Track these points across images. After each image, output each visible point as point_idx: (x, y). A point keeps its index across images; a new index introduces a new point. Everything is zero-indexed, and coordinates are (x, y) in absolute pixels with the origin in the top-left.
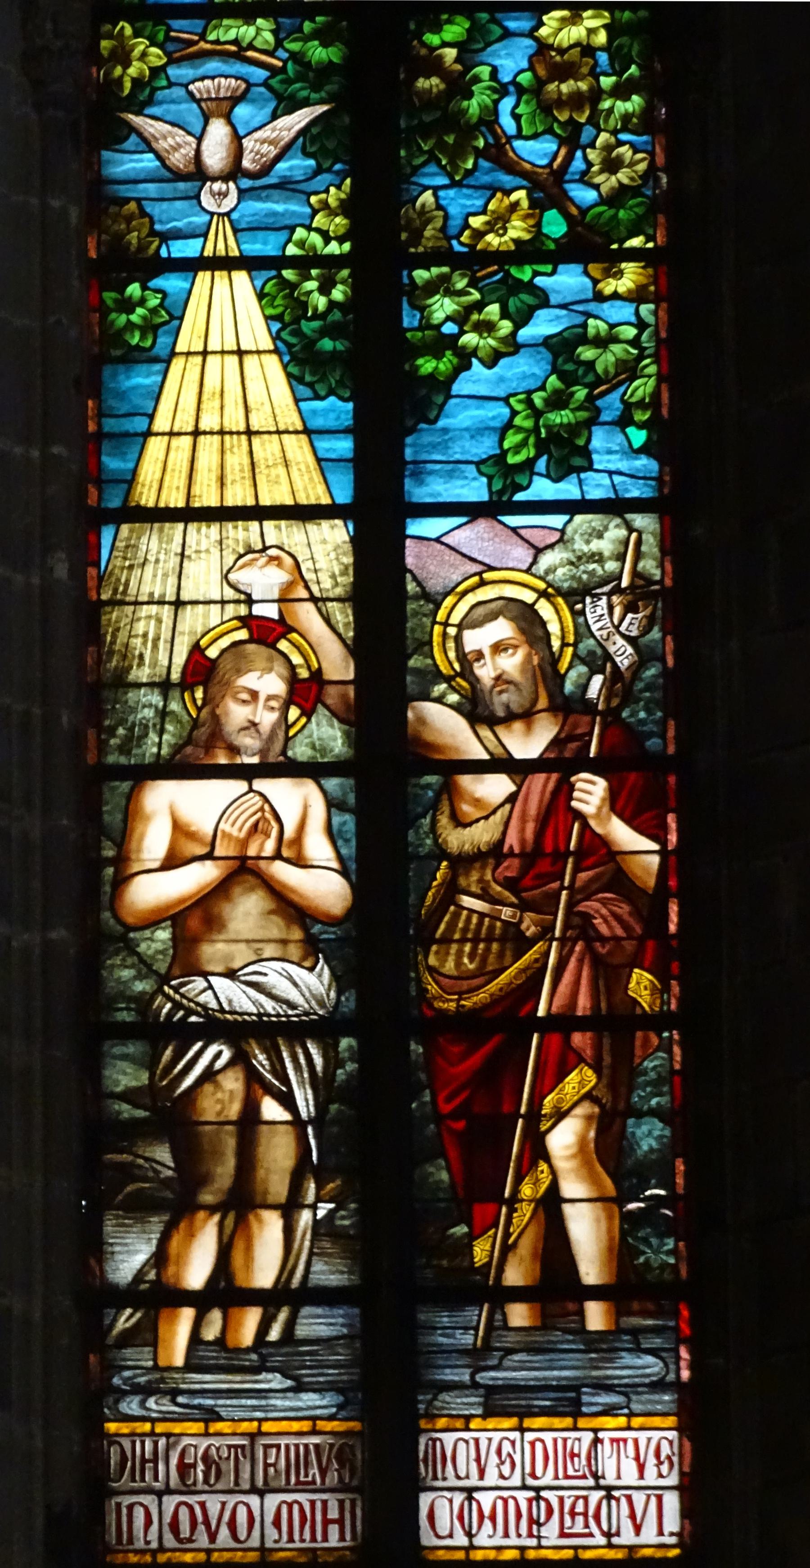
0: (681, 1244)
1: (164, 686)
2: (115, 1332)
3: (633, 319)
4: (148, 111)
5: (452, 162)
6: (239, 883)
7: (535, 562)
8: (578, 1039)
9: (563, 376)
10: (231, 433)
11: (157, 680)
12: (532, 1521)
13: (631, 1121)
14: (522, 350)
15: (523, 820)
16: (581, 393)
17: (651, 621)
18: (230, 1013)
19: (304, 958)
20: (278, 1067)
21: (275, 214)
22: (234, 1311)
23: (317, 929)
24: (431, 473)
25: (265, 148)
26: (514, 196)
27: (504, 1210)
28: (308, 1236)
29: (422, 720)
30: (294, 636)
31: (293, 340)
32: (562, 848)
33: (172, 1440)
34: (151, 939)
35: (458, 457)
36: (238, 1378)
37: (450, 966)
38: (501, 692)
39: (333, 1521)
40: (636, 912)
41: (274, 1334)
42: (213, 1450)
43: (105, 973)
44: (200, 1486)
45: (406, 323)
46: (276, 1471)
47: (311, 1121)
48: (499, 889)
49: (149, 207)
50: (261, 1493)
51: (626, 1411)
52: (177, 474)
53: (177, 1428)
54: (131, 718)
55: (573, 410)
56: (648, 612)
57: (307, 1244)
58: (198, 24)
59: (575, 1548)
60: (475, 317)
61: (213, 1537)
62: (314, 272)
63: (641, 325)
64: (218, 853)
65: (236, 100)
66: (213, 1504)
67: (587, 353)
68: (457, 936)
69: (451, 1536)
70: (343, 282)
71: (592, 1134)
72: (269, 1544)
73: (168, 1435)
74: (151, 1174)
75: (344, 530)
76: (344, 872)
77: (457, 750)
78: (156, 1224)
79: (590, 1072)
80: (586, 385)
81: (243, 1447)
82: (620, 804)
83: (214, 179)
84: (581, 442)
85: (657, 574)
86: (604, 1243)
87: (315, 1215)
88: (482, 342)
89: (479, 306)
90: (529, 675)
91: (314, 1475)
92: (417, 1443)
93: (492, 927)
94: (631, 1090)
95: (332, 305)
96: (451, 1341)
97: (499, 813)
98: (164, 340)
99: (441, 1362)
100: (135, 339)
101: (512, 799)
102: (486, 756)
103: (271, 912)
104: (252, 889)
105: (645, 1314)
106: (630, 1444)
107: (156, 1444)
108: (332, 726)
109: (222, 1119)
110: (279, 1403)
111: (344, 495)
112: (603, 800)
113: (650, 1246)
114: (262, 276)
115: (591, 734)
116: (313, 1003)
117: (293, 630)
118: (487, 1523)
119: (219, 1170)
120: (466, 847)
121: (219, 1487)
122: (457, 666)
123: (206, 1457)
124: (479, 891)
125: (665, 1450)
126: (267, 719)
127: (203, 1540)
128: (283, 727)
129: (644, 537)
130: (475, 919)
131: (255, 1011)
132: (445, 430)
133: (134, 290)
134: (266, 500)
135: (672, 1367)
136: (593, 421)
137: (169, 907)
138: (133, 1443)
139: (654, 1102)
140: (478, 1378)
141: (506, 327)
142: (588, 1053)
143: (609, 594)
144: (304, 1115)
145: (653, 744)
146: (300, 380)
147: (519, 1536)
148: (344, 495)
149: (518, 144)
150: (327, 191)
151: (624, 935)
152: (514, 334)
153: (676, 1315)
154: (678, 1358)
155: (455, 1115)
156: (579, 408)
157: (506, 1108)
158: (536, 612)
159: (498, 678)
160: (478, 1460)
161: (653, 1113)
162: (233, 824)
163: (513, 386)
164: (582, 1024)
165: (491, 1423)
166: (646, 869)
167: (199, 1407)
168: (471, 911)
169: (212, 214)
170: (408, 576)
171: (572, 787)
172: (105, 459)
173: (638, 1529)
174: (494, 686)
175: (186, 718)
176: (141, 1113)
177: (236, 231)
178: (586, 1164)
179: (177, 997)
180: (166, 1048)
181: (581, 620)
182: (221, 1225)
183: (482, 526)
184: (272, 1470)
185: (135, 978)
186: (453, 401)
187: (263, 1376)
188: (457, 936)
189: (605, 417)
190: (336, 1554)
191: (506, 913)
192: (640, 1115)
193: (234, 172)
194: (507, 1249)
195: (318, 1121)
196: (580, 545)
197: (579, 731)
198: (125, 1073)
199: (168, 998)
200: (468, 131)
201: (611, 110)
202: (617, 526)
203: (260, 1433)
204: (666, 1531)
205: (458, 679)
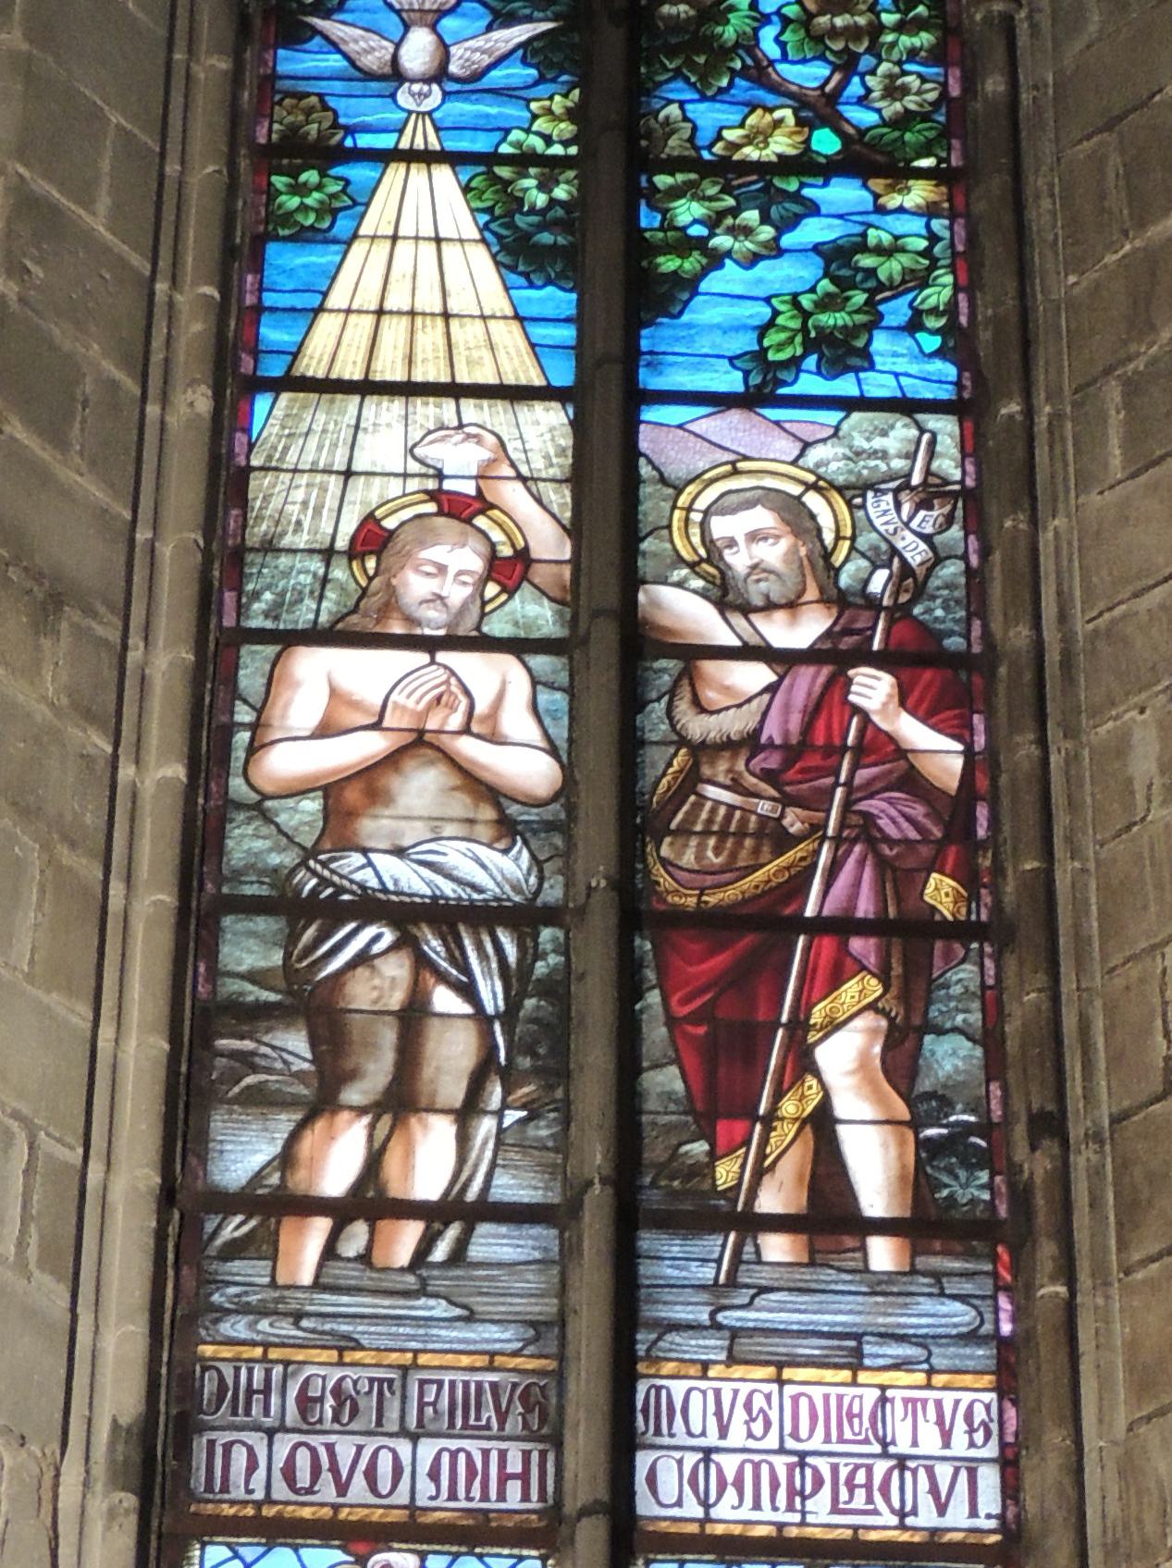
0: (998, 1179)
1: (328, 554)
2: (219, 1242)
3: (924, 232)
4: (335, 17)
6: (413, 757)
7: (802, 454)
8: (857, 945)
9: (835, 280)
10: (424, 314)
11: (317, 546)
13: (928, 1039)
14: (787, 256)
15: (787, 708)
16: (859, 298)
17: (949, 520)
18: (397, 893)
19: (498, 839)
20: (457, 954)
21: (488, 116)
22: (383, 1225)
23: (513, 809)
24: (671, 365)
25: (477, 56)
26: (778, 114)
27: (758, 1127)
28: (491, 1145)
29: (655, 603)
30: (495, 513)
31: (503, 232)
32: (837, 742)
33: (291, 1368)
34: (295, 810)
35: (705, 351)
36: (387, 1302)
37: (688, 859)
38: (758, 581)
39: (514, 1476)
40: (934, 814)
41: (440, 1252)
42: (348, 1384)
43: (230, 843)
44: (327, 1425)
45: (644, 223)
46: (435, 1411)
47: (498, 1016)
48: (754, 780)
49: (332, 102)
50: (414, 1438)
51: (925, 1366)
52: (354, 349)
53: (300, 1355)
54: (281, 584)
55: (850, 313)
56: (948, 508)
57: (488, 1154)
59: (856, 1528)
60: (729, 221)
61: (342, 1489)
62: (532, 171)
63: (933, 238)
64: (386, 724)
65: (442, 13)
66: (345, 1451)
67: (867, 261)
68: (699, 828)
69: (679, 1503)
70: (568, 182)
71: (877, 1049)
72: (419, 1503)
73: (287, 1363)
74: (279, 1065)
75: (562, 414)
76: (553, 751)
77: (700, 635)
78: (284, 1122)
79: (874, 982)
80: (865, 290)
81: (391, 1381)
82: (910, 702)
83: (413, 81)
84: (860, 343)
85: (957, 475)
86: (894, 1172)
87: (500, 1123)
88: (737, 245)
89: (735, 212)
90: (795, 566)
91: (489, 1419)
92: (633, 1391)
93: (744, 822)
94: (929, 1002)
95: (553, 202)
96: (684, 1274)
97: (755, 703)
98: (343, 226)
99: (669, 1298)
100: (310, 220)
101: (772, 689)
102: (736, 643)
103: (454, 789)
104: (432, 763)
106: (931, 1408)
107: (268, 1372)
108: (541, 605)
109: (376, 1008)
110: (443, 1333)
111: (563, 374)
112: (890, 696)
113: (956, 1177)
114: (466, 173)
115: (874, 628)
116: (507, 888)
117: (493, 506)
118: (731, 1493)
119: (371, 1067)
120: (712, 735)
121: (353, 1426)
122: (702, 552)
123: (337, 1391)
124: (728, 782)
125: (980, 1414)
126: (457, 594)
127: (327, 1491)
128: (478, 603)
129: (939, 438)
130: (722, 811)
131: (429, 892)
132: (689, 326)
133: (311, 176)
134: (463, 377)
135: (988, 1316)
136: (875, 323)
137: (317, 778)
138: (237, 1370)
139: (960, 1018)
140: (720, 1317)
141: (767, 232)
142: (872, 961)
143: (896, 492)
144: (490, 1009)
145: (954, 643)
146: (513, 269)
147: (775, 1509)
148: (563, 374)
149: (781, 67)
150: (551, 98)
151: (918, 837)
152: (776, 239)
153: (995, 1258)
154: (996, 1310)
155: (695, 1018)
156: (858, 311)
157: (761, 1015)
158: (804, 505)
159: (754, 567)
160: (719, 1413)
161: (956, 1030)
162: (409, 696)
163: (775, 288)
164: (863, 928)
165: (738, 1371)
166: (947, 770)
167: (331, 1333)
168: (718, 803)
169: (410, 112)
170: (642, 461)
171: (850, 682)
172: (263, 330)
173: (942, 1509)
174: (749, 575)
175: (353, 585)
176: (273, 997)
177: (437, 129)
178: (870, 1081)
179: (326, 873)
180: (305, 928)
181: (860, 513)
182: (372, 1127)
183: (735, 416)
184: (429, 1411)
185: (271, 850)
186: (699, 299)
187: (422, 1301)
188: (699, 828)
189: (890, 320)
190: (517, 1517)
191: (764, 807)
192: (940, 1032)
193: (440, 74)
194: (760, 1173)
195: (510, 1015)
196: (859, 442)
197: (859, 625)
198: (250, 952)
199: (314, 873)
200: (728, 52)
201: (893, 44)
202: (905, 426)
203: (415, 1366)
204: (982, 1511)
205: (705, 566)
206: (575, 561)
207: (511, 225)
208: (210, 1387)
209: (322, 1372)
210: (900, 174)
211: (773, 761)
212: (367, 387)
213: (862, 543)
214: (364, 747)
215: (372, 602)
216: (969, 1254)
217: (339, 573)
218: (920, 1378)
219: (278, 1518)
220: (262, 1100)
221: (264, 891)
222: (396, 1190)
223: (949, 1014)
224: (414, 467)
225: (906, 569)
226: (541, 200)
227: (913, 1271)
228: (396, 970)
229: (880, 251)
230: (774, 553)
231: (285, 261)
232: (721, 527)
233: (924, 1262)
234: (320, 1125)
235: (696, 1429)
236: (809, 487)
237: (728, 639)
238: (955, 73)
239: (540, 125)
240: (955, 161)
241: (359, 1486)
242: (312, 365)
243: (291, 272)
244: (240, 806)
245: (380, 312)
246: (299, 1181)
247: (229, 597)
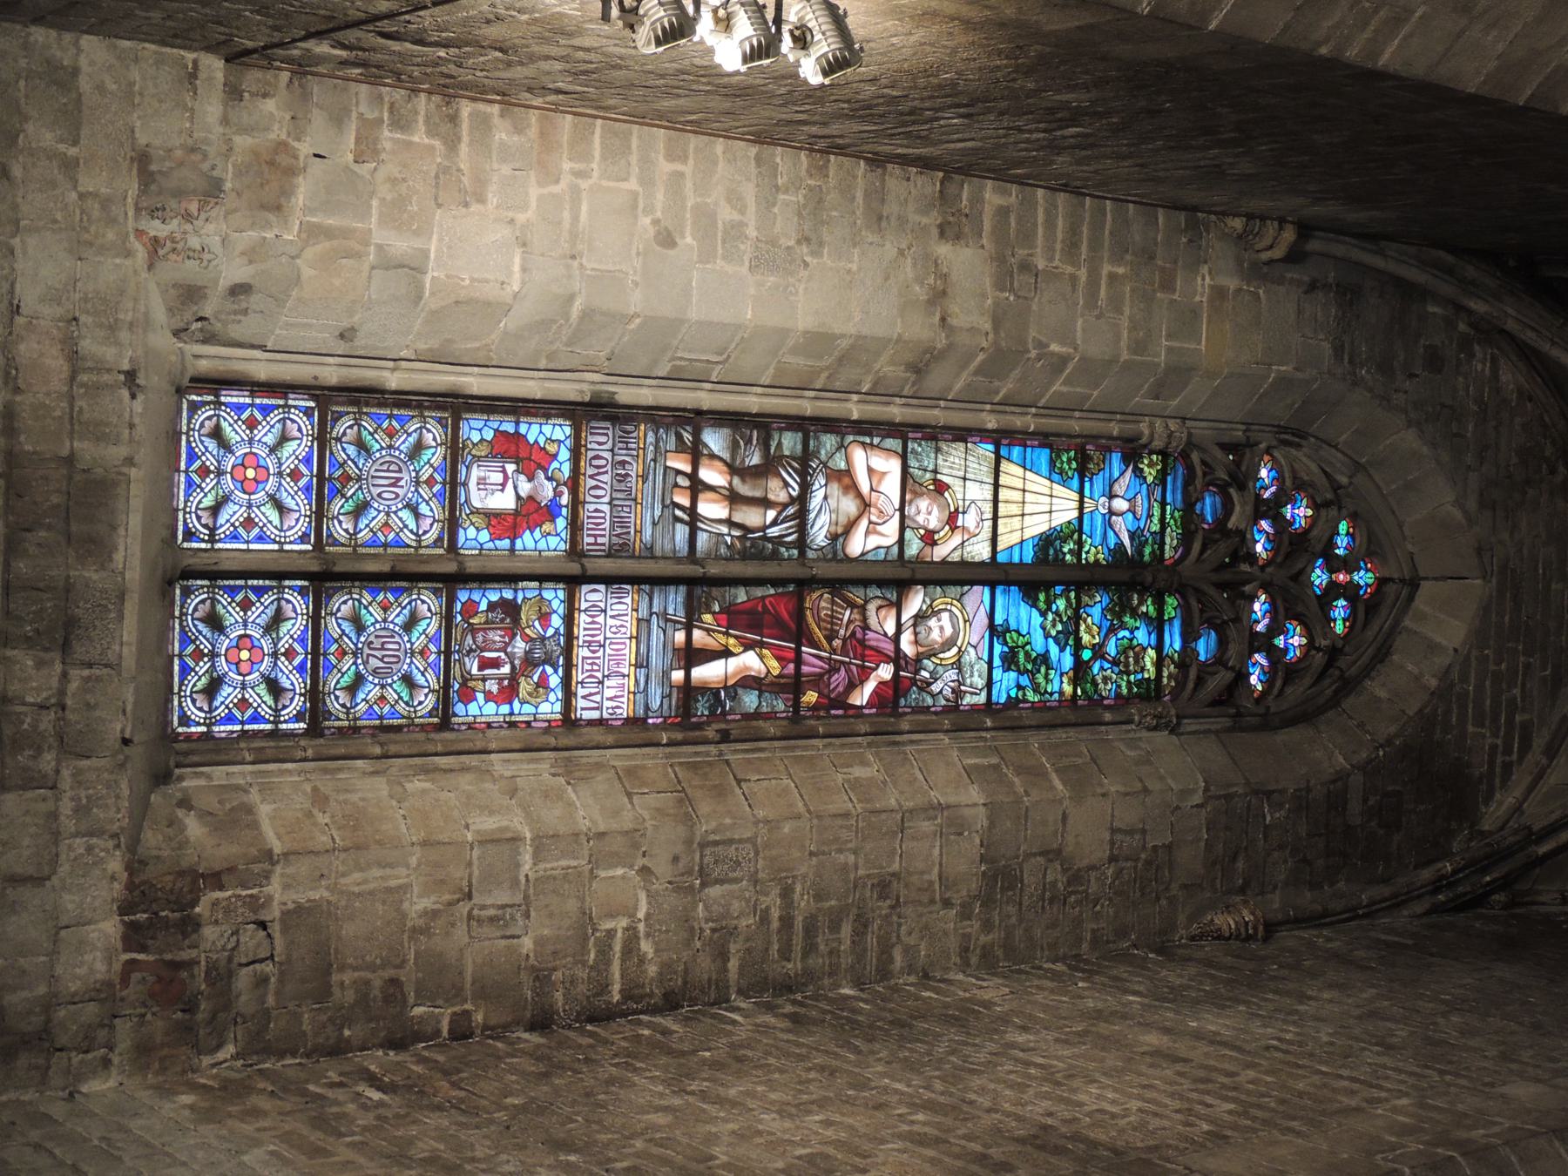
1: (935, 471)
5: (1110, 610)
8: (791, 666)
12: (590, 642)
15: (878, 640)
16: (1029, 667)
17: (948, 700)
23: (841, 540)
29: (917, 592)
37: (823, 604)
40: (840, 694)
41: (678, 513)
50: (610, 503)
53: (640, 461)
58: (1159, 499)
61: (591, 477)
63: (1051, 694)
65: (1134, 513)
66: (606, 478)
67: (1043, 670)
76: (863, 554)
78: (726, 456)
89: (1061, 621)
93: (837, 624)
95: (1064, 554)
98: (1056, 477)
100: (1058, 465)
101: (885, 635)
105: (678, 698)
111: (1001, 558)
114: (1075, 522)
118: (590, 620)
125: (619, 711)
126: (920, 519)
127: (590, 471)
133: (1074, 465)
134: (1000, 521)
136: (1020, 673)
141: (1053, 633)
142: (785, 671)
145: (902, 702)
148: (1001, 558)
153: (676, 717)
155: (764, 606)
164: (798, 668)
165: (635, 622)
173: (584, 697)
176: (772, 451)
178: (741, 671)
182: (724, 488)
183: (986, 621)
189: (1021, 678)
191: (842, 632)
192: (759, 697)
193: (1111, 512)
194: (707, 630)
195: (765, 538)
196: (976, 667)
200: (1120, 618)
206: (932, 562)
207: (1056, 539)
208: (629, 428)
209: (634, 469)
210: (1075, 682)
211: (859, 635)
212: (996, 486)
213: (939, 668)
214: (864, 485)
215: (917, 487)
216: (678, 707)
217: (928, 475)
218: (632, 689)
219: (580, 453)
220: (734, 447)
221: (811, 448)
222: (701, 496)
223: (766, 700)
224: (967, 503)
225: (929, 684)
226: (1066, 550)
227: (671, 687)
228: (782, 497)
229: (1047, 675)
230: (935, 635)
231: (1043, 456)
232: (945, 616)
233: (675, 690)
234: (725, 469)
235: (614, 607)
236: (960, 648)
237: (904, 619)
238: (1112, 702)
239: (1093, 549)
240: (1080, 702)
241: (592, 483)
242: (1004, 466)
243: (1039, 458)
244: (842, 439)
245: (1024, 491)
246: (704, 461)
247: (919, 435)
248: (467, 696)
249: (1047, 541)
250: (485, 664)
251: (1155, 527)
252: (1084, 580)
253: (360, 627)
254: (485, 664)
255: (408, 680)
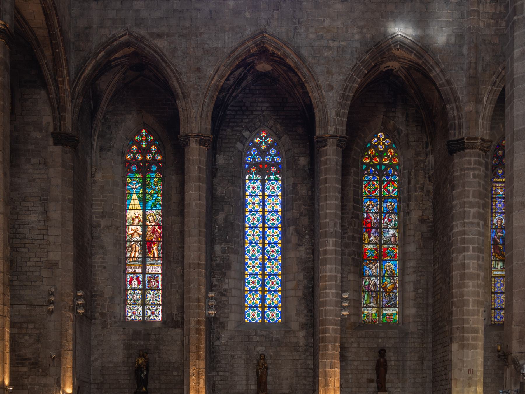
193: (135, 188)
209: (132, 266)
214: (133, 232)
220: (129, 252)
228: (135, 244)
230: (152, 219)
231: (128, 201)
242: (130, 208)
248: (158, 287)
249: (140, 200)
250: (154, 285)
251: (137, 179)
252: (144, 193)
253: (150, 300)
254: (154, 285)
255: (156, 294)
